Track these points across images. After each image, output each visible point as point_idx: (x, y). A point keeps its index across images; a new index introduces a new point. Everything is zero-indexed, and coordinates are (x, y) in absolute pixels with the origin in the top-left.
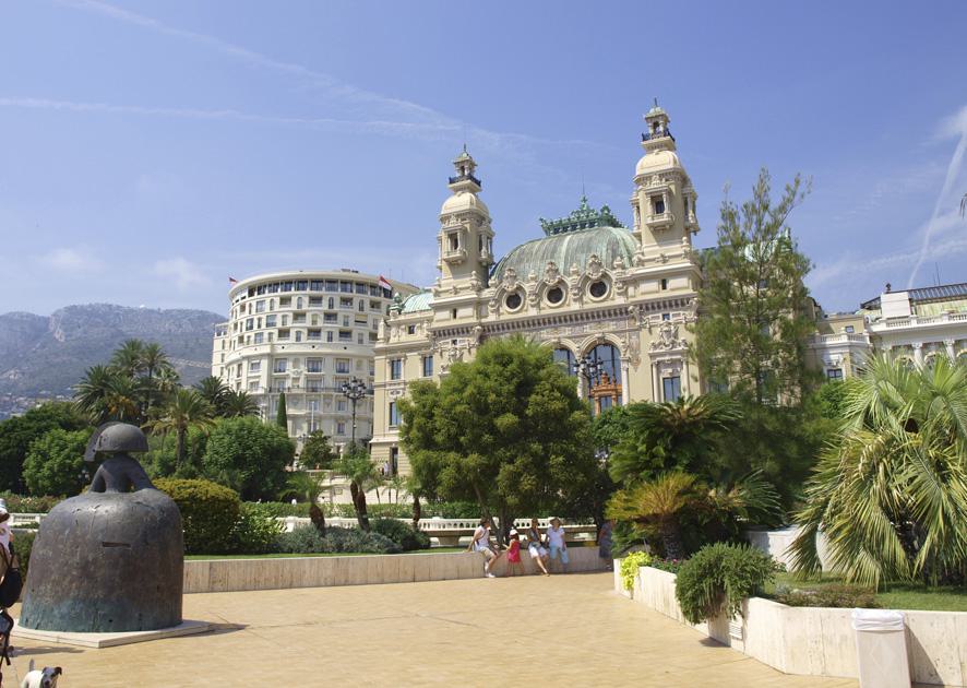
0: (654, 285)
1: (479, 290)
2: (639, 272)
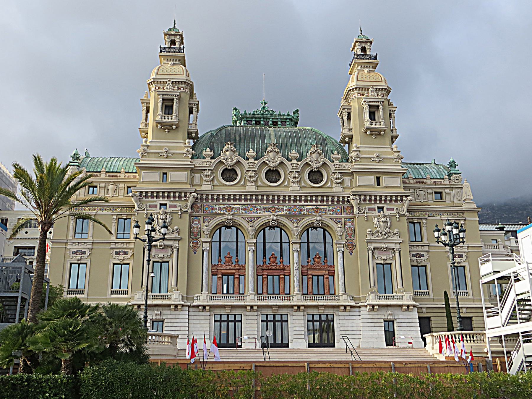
2: (355, 167)
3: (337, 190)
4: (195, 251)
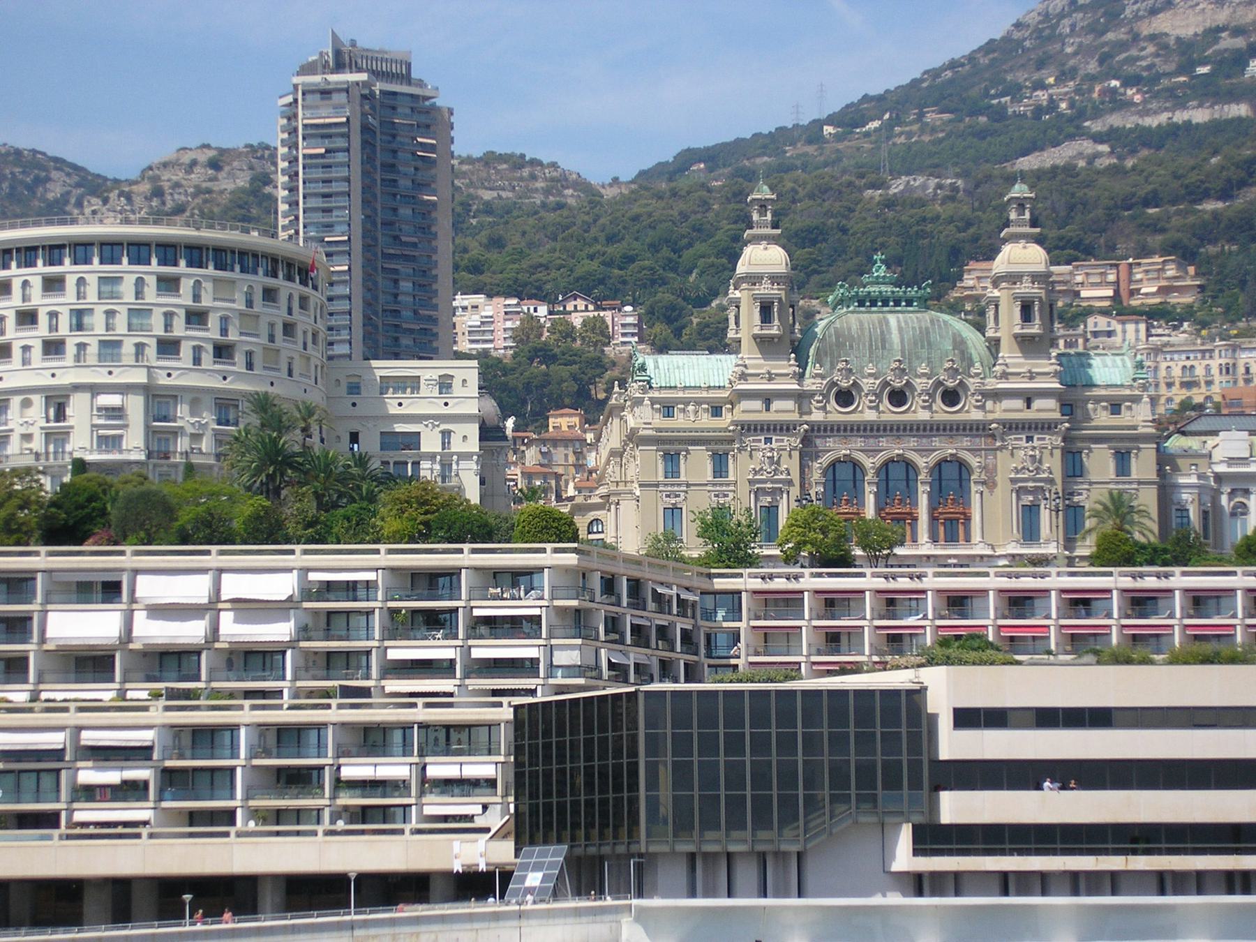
0: (1019, 403)
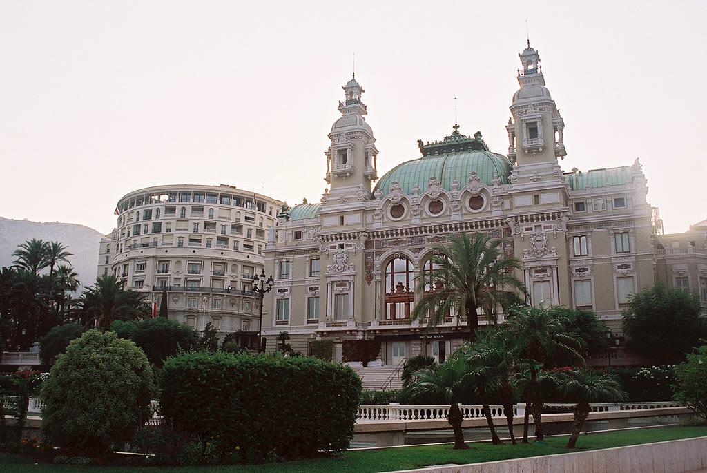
1: (366, 200)
3: (497, 213)
4: (369, 283)
